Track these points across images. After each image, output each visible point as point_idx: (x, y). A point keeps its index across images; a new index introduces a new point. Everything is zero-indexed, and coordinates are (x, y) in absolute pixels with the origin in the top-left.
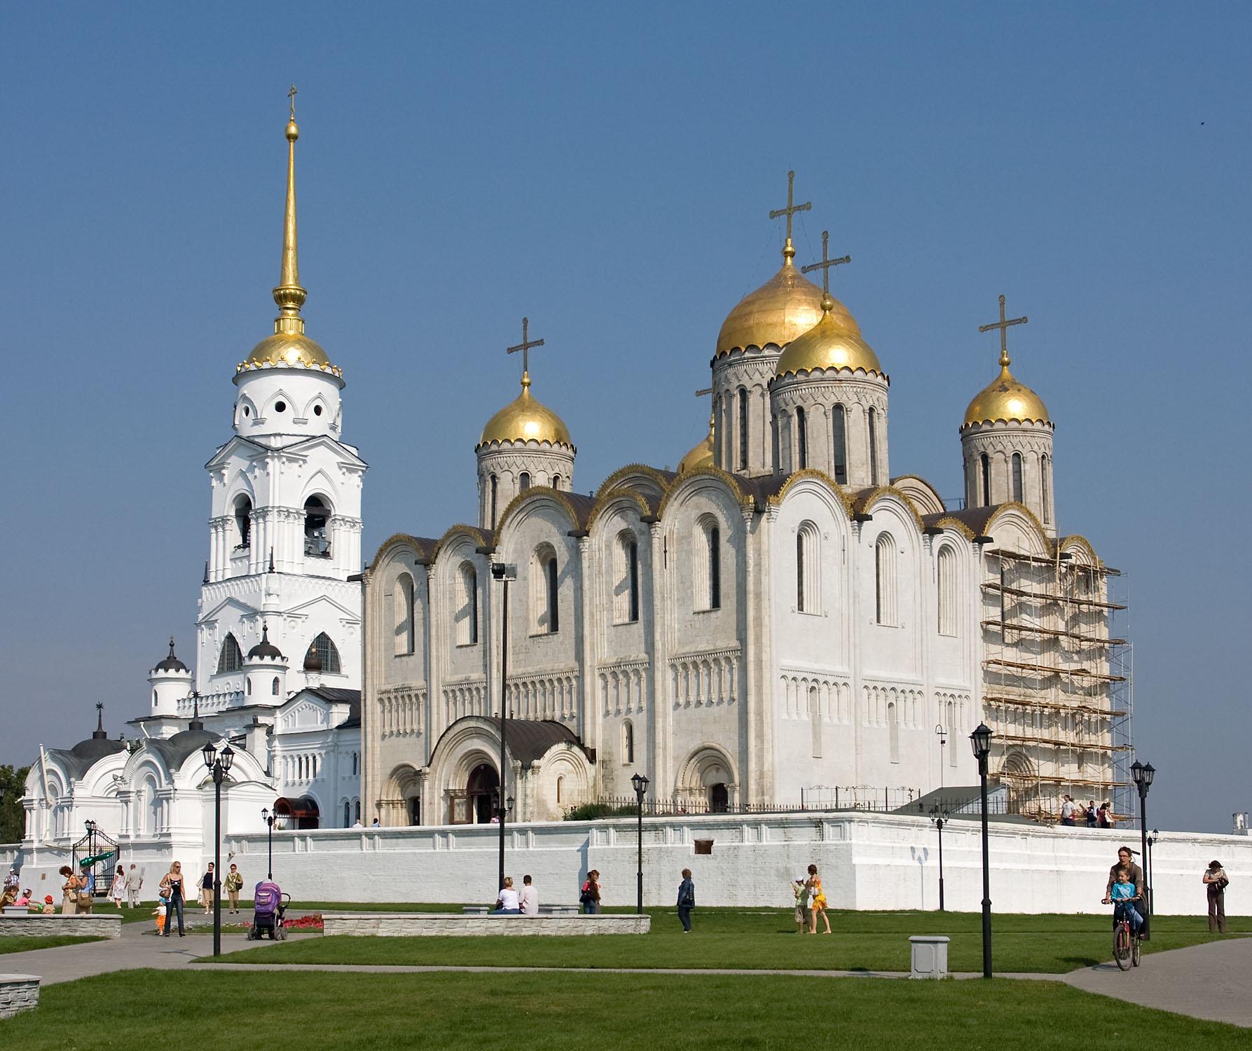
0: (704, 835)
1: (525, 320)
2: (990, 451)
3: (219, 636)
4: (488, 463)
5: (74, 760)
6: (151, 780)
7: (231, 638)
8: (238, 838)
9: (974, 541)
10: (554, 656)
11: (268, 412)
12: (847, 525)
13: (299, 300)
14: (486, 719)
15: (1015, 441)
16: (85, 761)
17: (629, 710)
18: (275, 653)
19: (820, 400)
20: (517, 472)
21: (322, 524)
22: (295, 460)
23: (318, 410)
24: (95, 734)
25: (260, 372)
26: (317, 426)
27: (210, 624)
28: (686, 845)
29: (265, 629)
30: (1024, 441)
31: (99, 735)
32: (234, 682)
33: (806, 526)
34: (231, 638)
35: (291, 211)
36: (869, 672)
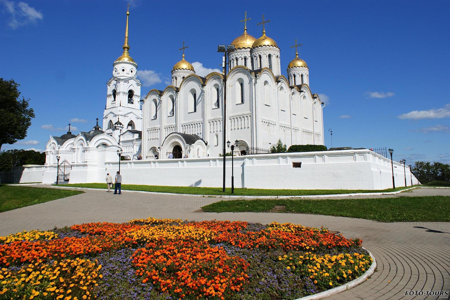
0: (297, 160)
2: (296, 74)
3: (108, 120)
4: (174, 75)
5: (61, 140)
6: (82, 145)
7: (111, 121)
12: (275, 83)
13: (128, 48)
16: (64, 140)
17: (217, 131)
18: (121, 124)
23: (132, 71)
24: (68, 133)
25: (119, 63)
27: (106, 118)
28: (289, 164)
31: (69, 133)
33: (266, 83)
35: (127, 29)
36: (280, 122)
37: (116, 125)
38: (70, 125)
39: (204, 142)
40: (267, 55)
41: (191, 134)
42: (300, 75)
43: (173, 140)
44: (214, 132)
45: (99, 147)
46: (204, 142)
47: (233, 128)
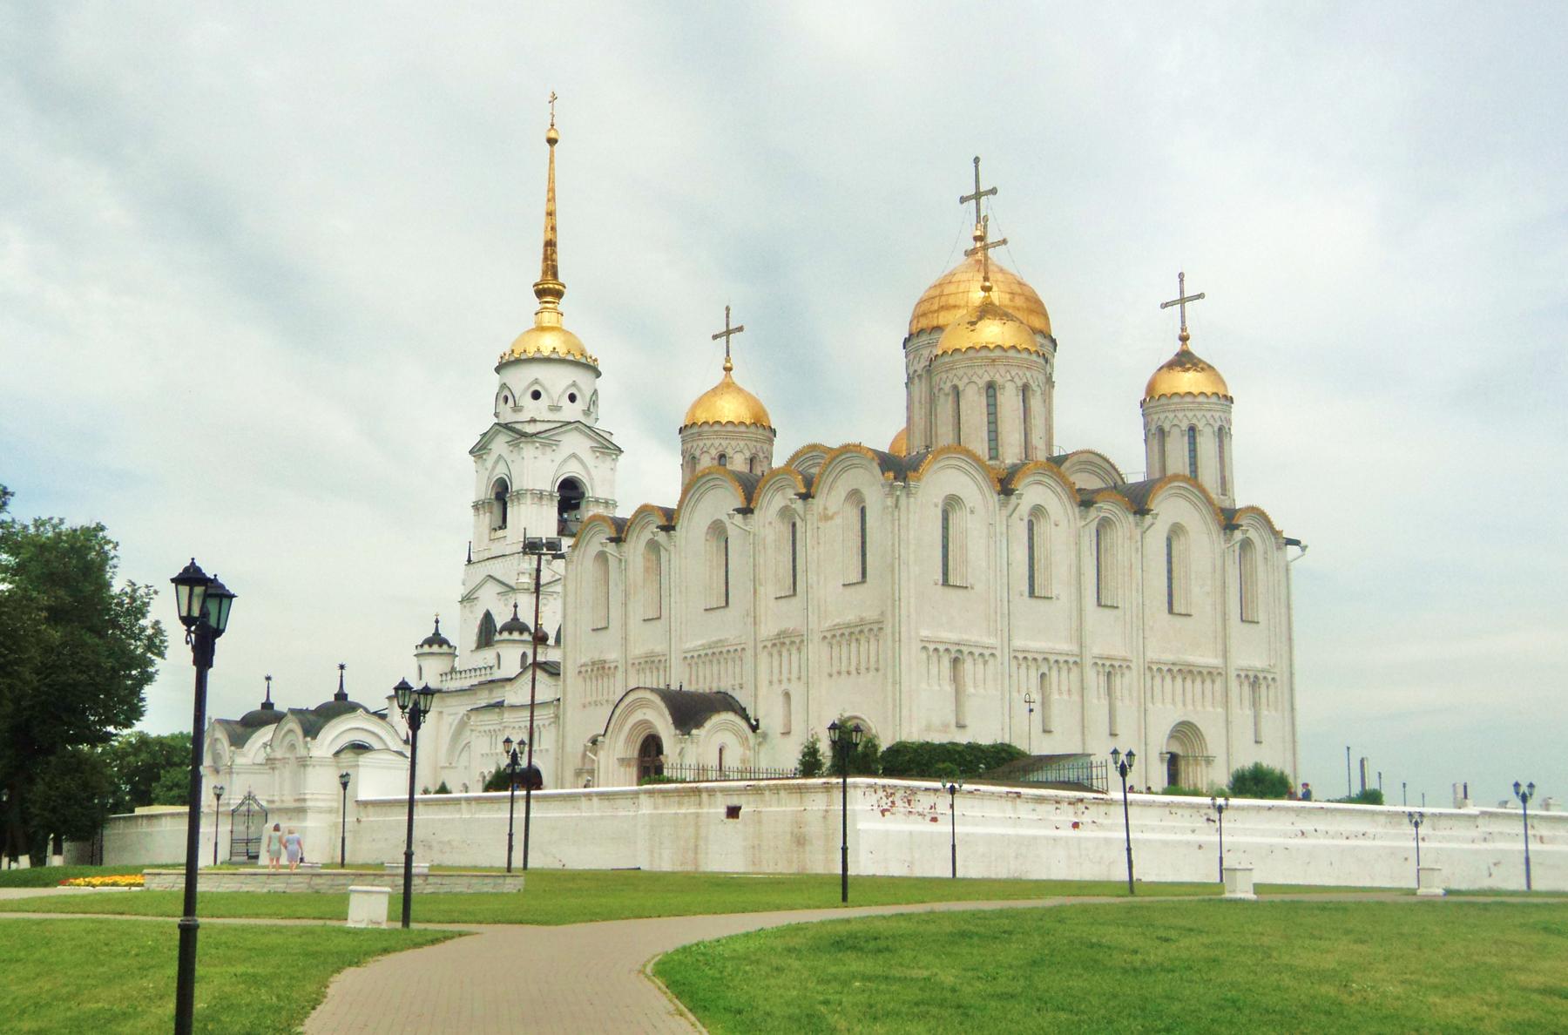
0: (734, 801)
1: (728, 309)
5: (239, 729)
8: (365, 804)
9: (1135, 513)
10: (728, 627)
12: (994, 499)
14: (652, 690)
15: (1190, 414)
19: (975, 378)
20: (714, 452)
21: (577, 507)
22: (550, 445)
23: (572, 398)
26: (571, 412)
29: (516, 606)
30: (1199, 414)
31: (268, 705)
32: (488, 656)
33: (951, 504)
34: (488, 617)
36: (1018, 643)
37: (505, 635)
38: (268, 678)
39: (747, 719)
40: (982, 383)
41: (715, 689)
42: (1185, 426)
43: (639, 716)
44: (780, 681)
45: (342, 755)
46: (747, 719)
47: (835, 670)
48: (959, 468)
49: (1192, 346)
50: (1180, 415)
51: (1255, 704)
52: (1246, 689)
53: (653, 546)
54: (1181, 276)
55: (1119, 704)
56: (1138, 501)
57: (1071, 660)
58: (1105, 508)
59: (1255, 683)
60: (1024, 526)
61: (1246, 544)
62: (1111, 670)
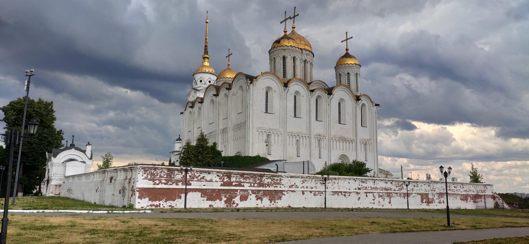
11: (198, 82)
15: (348, 70)
36: (289, 129)
48: (271, 79)
49: (349, 52)
50: (345, 70)
51: (365, 150)
52: (362, 145)
53: (200, 109)
54: (347, 33)
55: (322, 150)
56: (330, 91)
57: (307, 136)
58: (317, 93)
59: (365, 145)
60: (293, 96)
61: (363, 105)
62: (319, 139)
